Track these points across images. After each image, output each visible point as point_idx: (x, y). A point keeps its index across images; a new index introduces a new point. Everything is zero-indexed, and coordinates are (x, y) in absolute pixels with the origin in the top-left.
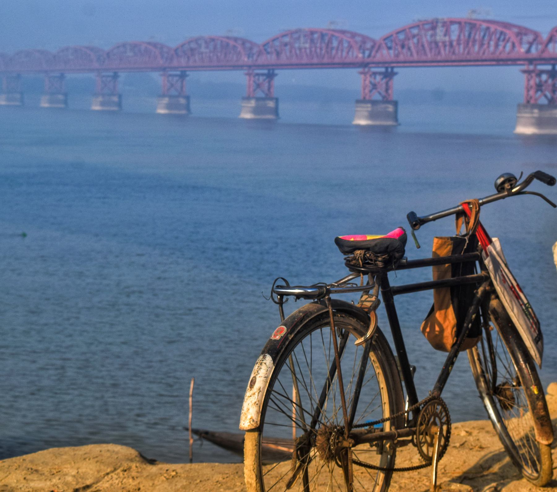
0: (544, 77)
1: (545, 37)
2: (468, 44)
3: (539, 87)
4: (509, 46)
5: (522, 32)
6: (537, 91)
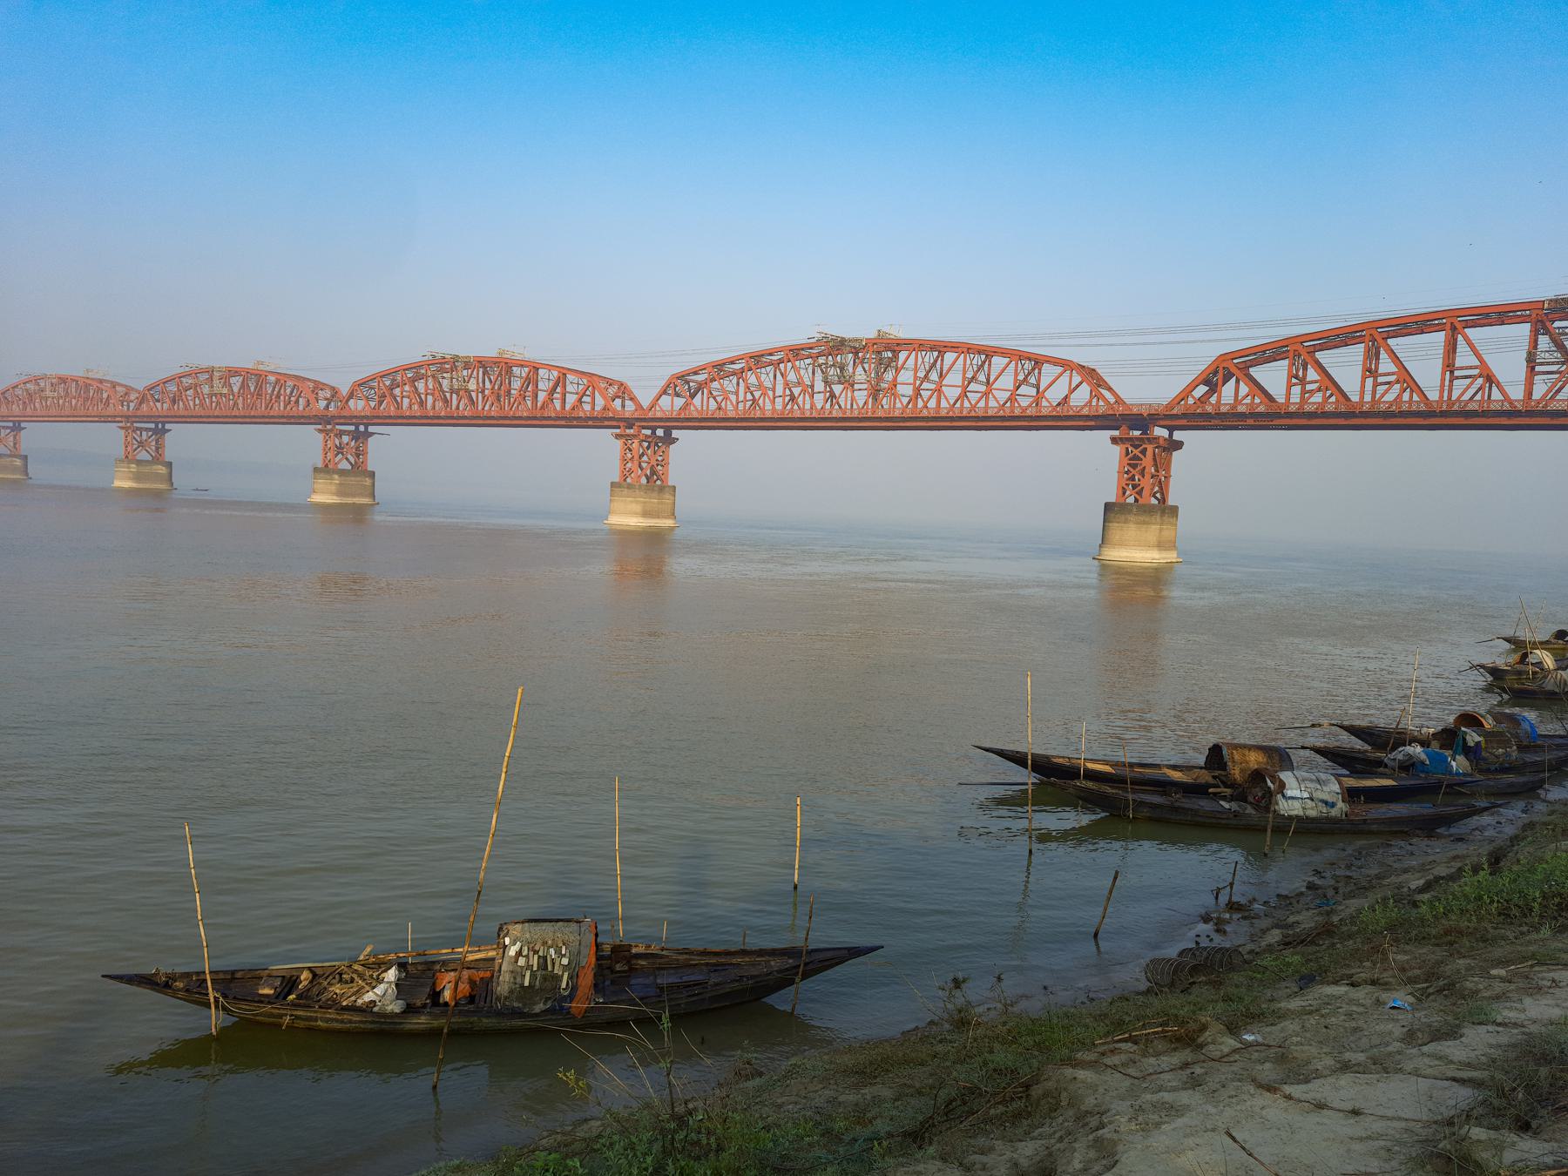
0: (345, 439)
1: (345, 391)
5: (318, 386)
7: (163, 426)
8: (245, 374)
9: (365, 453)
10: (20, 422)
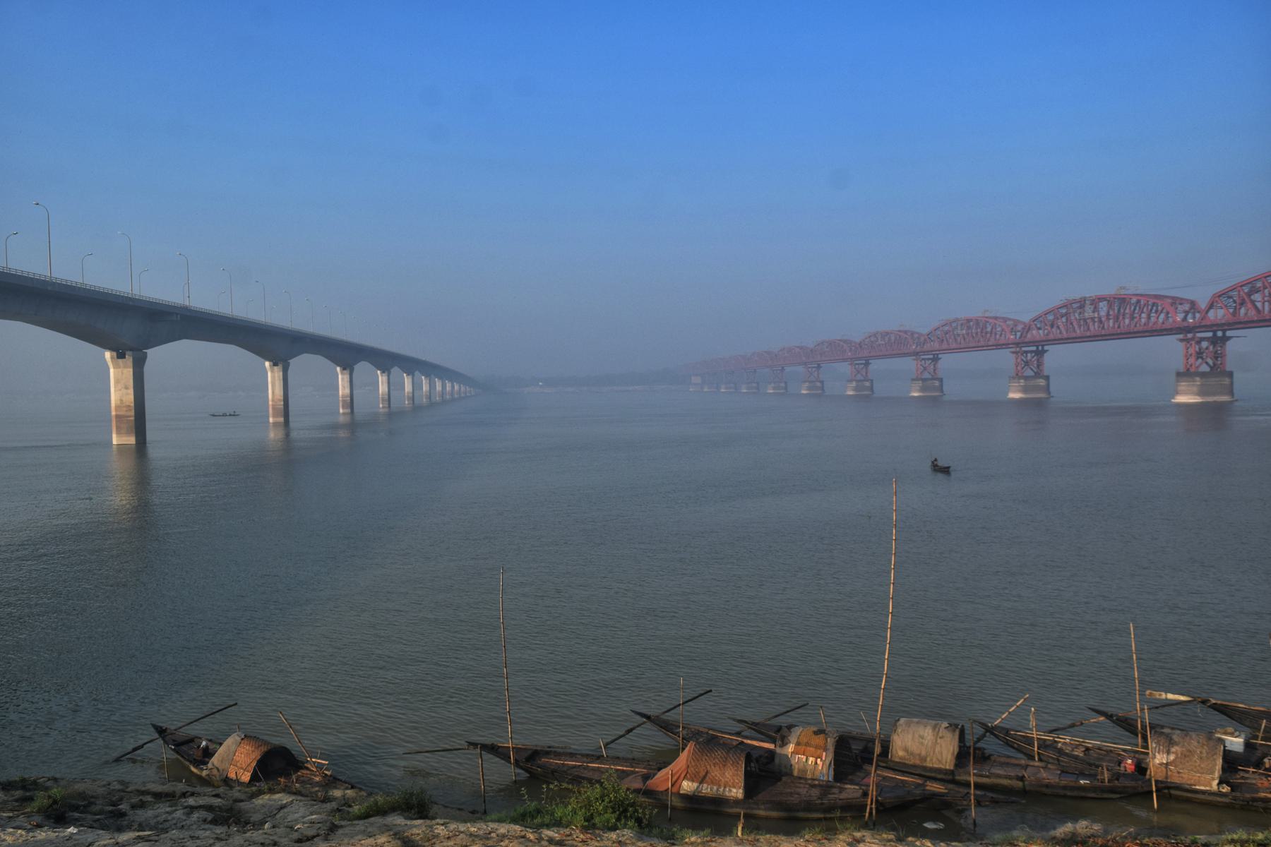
0: (1205, 344)
2: (1118, 318)
3: (1199, 354)
4: (1162, 316)
5: (1176, 301)
6: (1198, 358)
7: (1043, 348)
8: (1110, 300)
9: (1223, 355)
10: (938, 354)
